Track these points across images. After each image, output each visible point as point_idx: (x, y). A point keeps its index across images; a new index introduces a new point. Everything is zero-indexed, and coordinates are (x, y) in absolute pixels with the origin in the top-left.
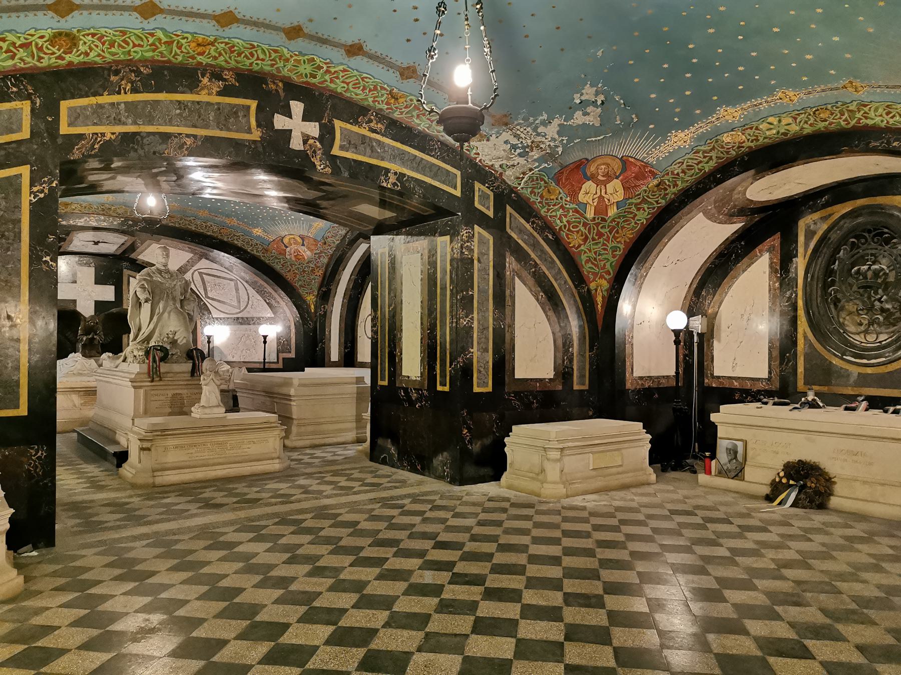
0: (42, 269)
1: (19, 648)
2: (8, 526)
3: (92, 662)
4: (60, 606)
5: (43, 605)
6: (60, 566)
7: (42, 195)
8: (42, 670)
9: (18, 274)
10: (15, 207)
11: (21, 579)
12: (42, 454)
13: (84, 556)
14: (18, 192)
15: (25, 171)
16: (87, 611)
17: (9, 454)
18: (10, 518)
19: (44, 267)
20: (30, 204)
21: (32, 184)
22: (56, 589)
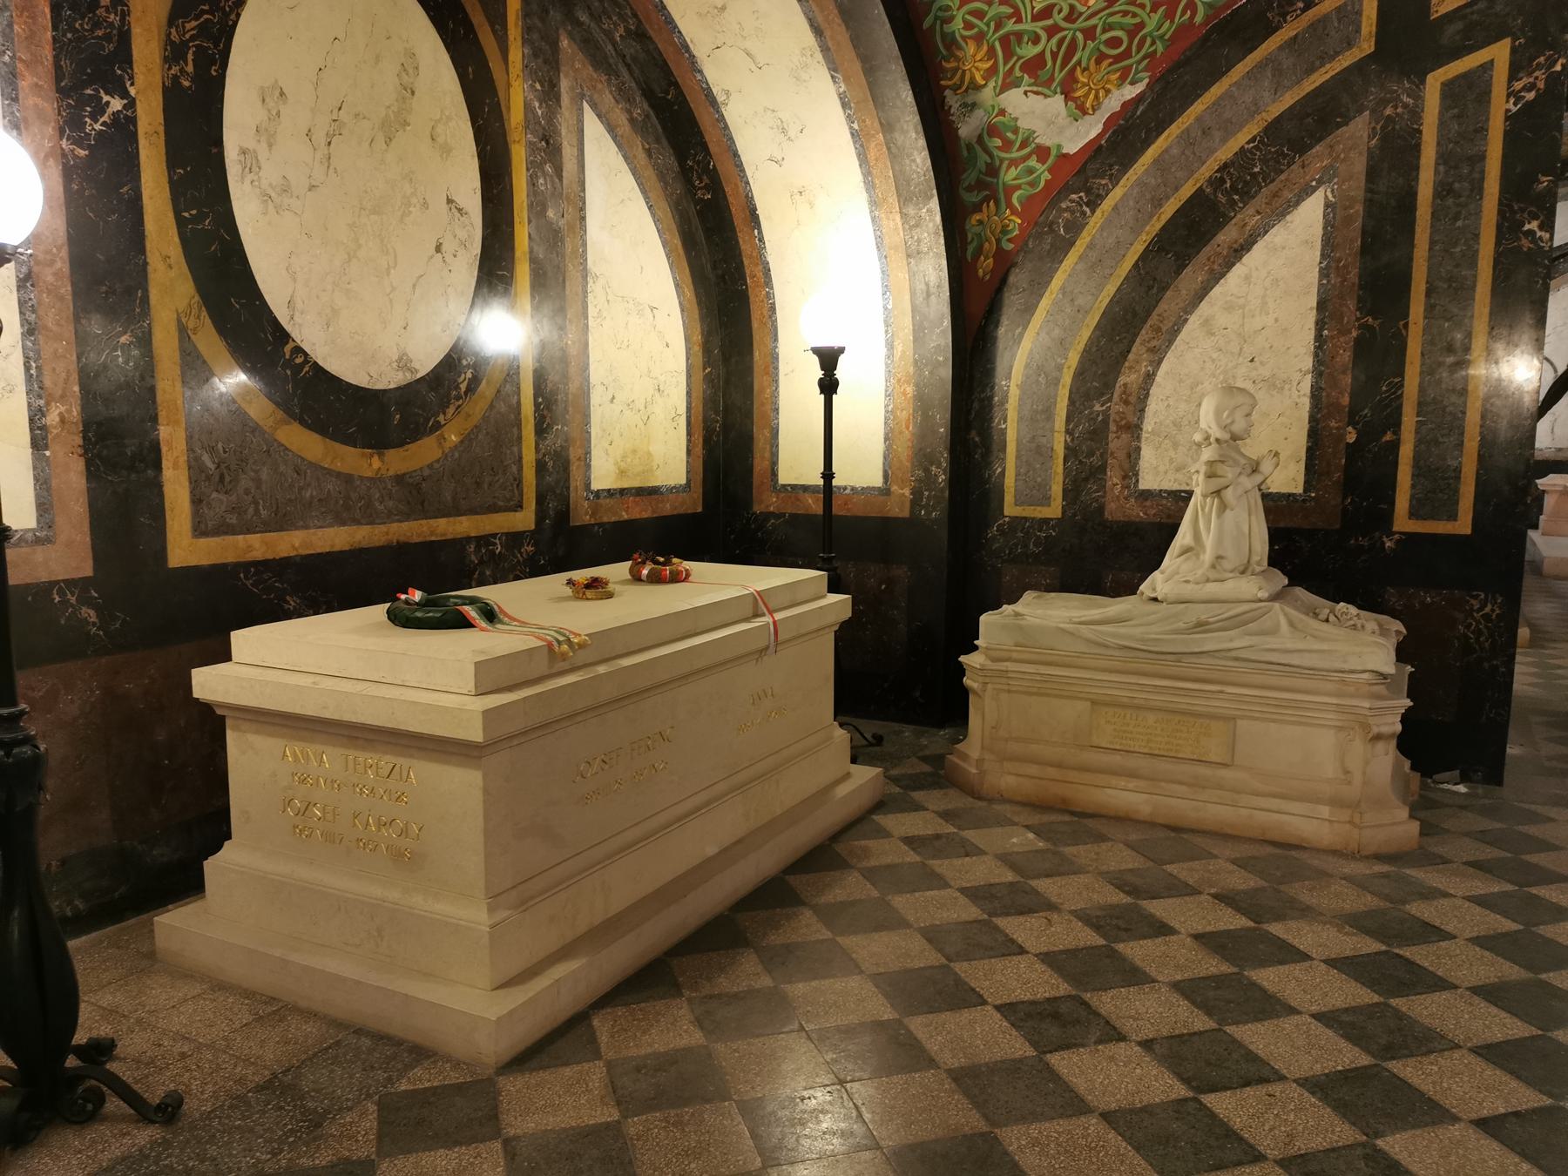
0: (1520, 247)
1: (1372, 946)
2: (1399, 728)
3: (1489, 1027)
4: (1469, 899)
5: (1440, 886)
6: (1498, 825)
7: (1531, 96)
8: (1394, 1002)
9: (1473, 263)
10: (1476, 131)
11: (1415, 827)
12: (1493, 610)
13: (1551, 820)
14: (1484, 97)
15: (1499, 53)
16: (1515, 927)
17: (1433, 602)
18: (1403, 714)
19: (1525, 243)
20: (1507, 118)
21: (1513, 76)
22: (1477, 865)
